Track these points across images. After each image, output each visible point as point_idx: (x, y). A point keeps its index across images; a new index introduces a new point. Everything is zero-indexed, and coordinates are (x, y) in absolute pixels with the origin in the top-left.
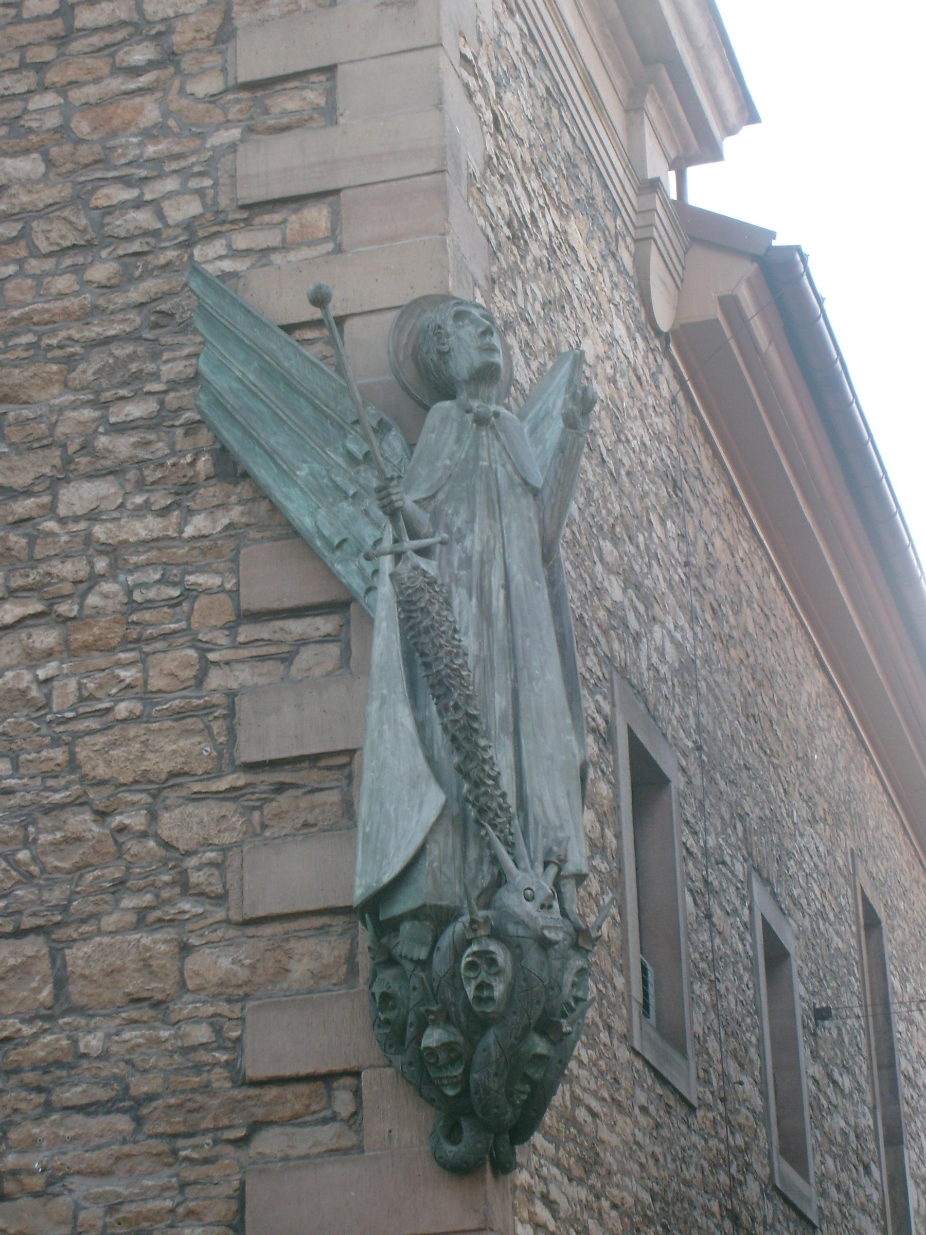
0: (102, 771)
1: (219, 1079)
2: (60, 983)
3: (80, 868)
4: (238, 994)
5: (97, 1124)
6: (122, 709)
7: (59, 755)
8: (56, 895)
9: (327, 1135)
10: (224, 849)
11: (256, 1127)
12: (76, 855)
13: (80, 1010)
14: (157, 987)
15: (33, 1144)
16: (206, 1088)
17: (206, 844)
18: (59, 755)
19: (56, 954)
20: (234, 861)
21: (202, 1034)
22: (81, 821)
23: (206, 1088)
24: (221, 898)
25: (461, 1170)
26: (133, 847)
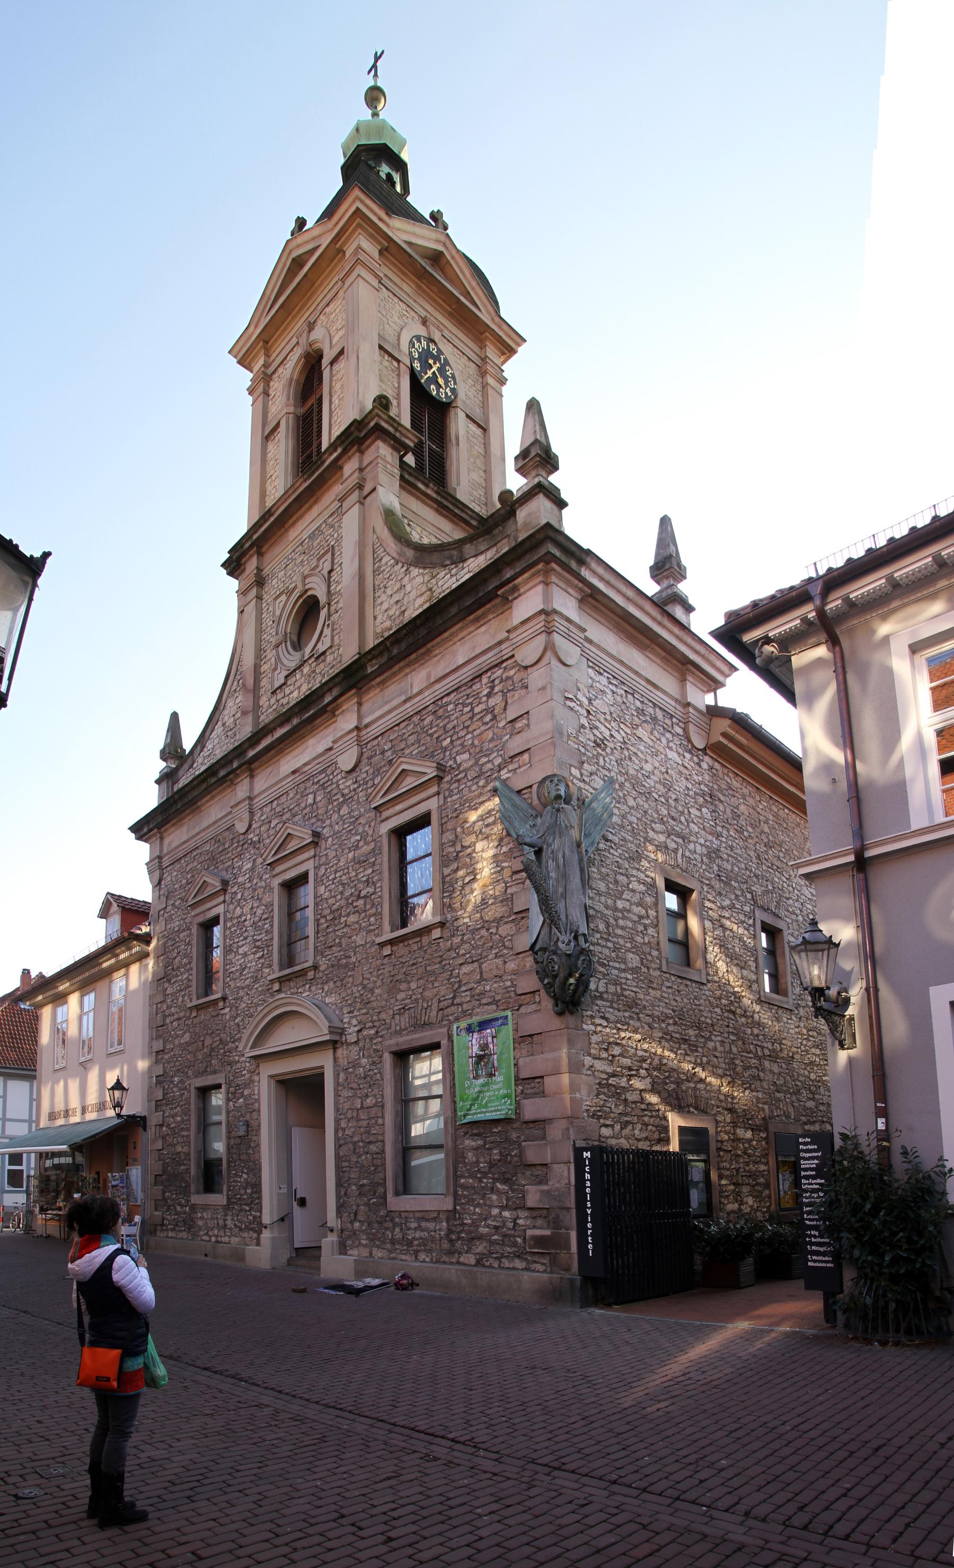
0: (487, 919)
1: (512, 994)
2: (481, 973)
3: (484, 944)
4: (515, 973)
5: (489, 1007)
6: (490, 902)
7: (478, 915)
8: (479, 951)
9: (534, 1007)
10: (512, 936)
11: (520, 1006)
12: (483, 940)
13: (485, 980)
14: (500, 973)
15: (477, 1014)
16: (510, 997)
17: (508, 935)
18: (478, 915)
19: (480, 967)
20: (514, 938)
21: (509, 983)
22: (484, 932)
23: (510, 997)
24: (512, 948)
25: (560, 1014)
26: (494, 937)
